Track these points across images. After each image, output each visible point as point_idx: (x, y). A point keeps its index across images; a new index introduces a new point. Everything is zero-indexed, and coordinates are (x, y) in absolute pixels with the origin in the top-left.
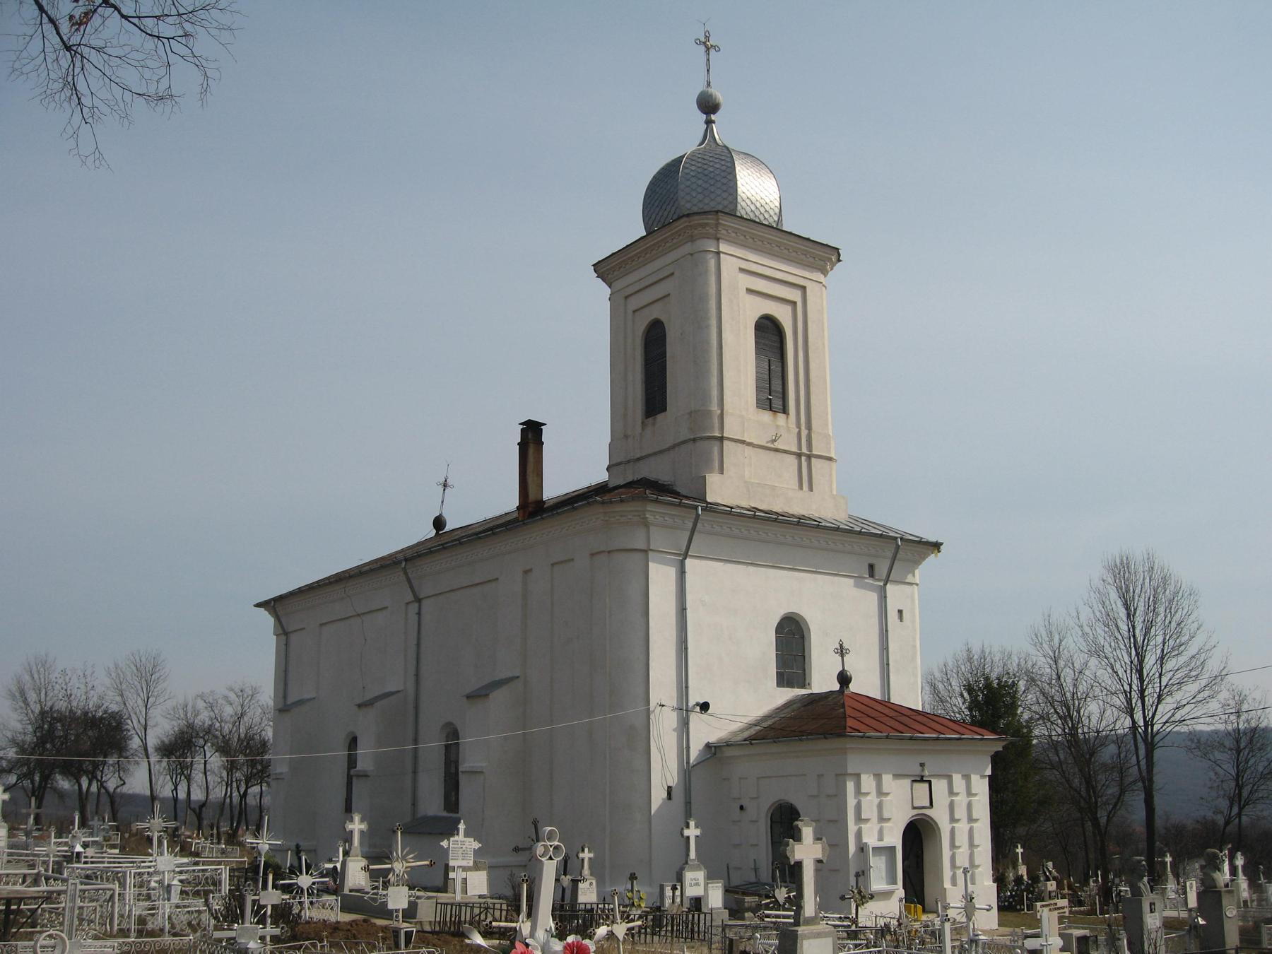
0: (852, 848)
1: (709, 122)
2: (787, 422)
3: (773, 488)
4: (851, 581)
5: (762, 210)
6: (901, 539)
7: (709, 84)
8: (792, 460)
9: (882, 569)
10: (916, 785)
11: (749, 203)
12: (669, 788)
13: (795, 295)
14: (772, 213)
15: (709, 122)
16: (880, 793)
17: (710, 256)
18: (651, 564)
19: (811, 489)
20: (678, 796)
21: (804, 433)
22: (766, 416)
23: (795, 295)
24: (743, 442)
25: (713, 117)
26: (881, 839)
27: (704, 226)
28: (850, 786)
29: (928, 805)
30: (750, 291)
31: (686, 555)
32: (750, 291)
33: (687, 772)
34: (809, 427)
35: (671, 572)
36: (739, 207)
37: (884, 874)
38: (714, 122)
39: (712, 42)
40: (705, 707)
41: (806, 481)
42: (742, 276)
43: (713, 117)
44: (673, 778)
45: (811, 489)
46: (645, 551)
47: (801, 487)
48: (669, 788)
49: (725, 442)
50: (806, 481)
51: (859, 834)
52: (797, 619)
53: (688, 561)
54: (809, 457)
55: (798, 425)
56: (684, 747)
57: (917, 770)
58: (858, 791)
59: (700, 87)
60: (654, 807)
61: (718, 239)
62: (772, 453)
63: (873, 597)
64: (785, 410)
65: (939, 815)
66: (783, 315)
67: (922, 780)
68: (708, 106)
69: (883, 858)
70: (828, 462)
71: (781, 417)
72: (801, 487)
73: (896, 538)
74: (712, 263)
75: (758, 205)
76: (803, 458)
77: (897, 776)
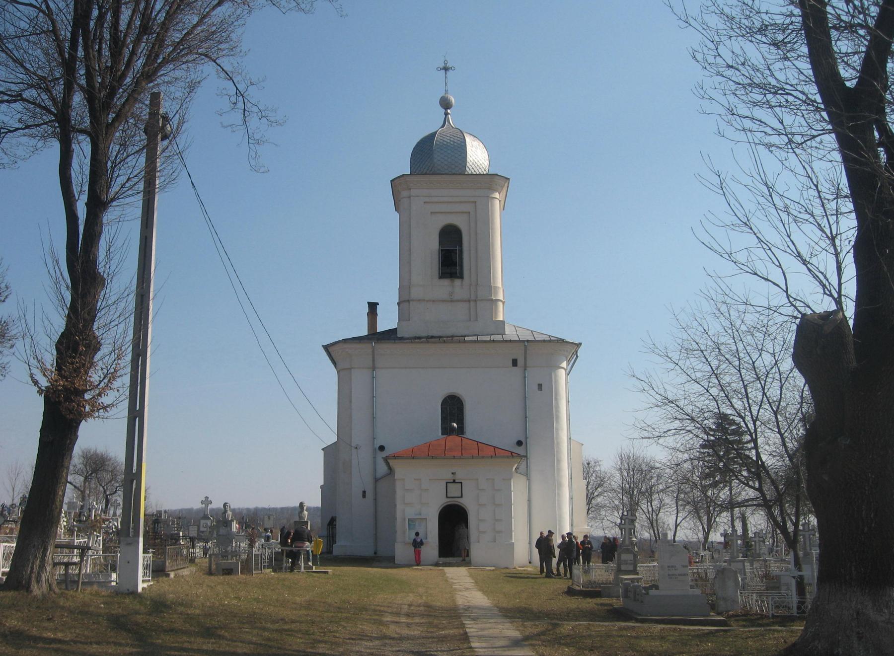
1: (446, 114)
2: (462, 283)
7: (446, 91)
9: (520, 362)
15: (446, 114)
20: (369, 494)
22: (446, 282)
25: (449, 111)
29: (460, 495)
31: (374, 368)
38: (449, 114)
40: (382, 448)
43: (449, 111)
46: (350, 369)
49: (411, 302)
52: (458, 396)
54: (475, 301)
57: (450, 477)
59: (443, 94)
61: (410, 189)
65: (467, 502)
66: (459, 221)
67: (454, 482)
68: (446, 104)
71: (457, 282)
76: (471, 302)
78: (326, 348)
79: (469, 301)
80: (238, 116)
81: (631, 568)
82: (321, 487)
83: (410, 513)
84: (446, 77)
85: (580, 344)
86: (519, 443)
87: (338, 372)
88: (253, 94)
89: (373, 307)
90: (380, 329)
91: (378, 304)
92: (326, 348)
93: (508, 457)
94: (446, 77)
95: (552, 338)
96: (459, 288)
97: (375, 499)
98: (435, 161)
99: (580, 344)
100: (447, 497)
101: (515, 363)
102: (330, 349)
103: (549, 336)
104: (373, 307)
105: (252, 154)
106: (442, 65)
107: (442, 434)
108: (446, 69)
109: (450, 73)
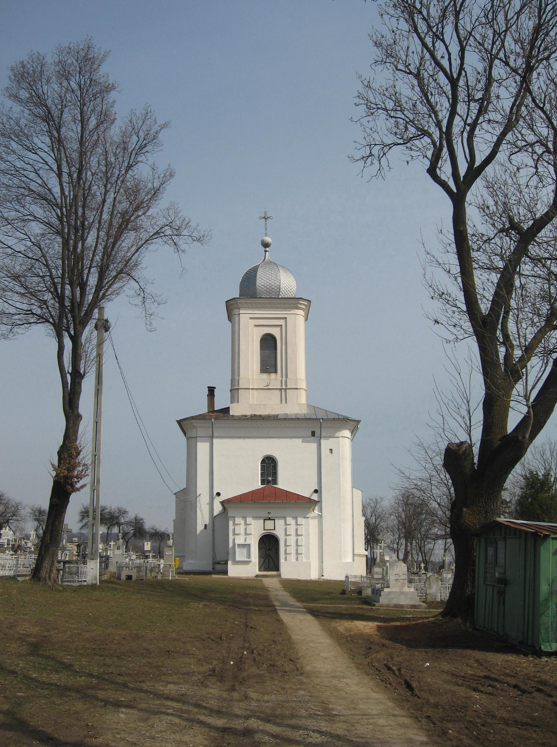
0: (231, 545)
3: (265, 405)
4: (300, 440)
5: (270, 288)
6: (322, 419)
8: (278, 392)
9: (317, 433)
10: (266, 522)
11: (263, 287)
12: (206, 525)
13: (282, 322)
14: (276, 288)
16: (246, 524)
17: (236, 316)
18: (198, 443)
19: (286, 403)
20: (209, 528)
21: (284, 379)
22: (265, 376)
23: (282, 322)
24: (249, 389)
25: (267, 249)
26: (245, 541)
27: (233, 304)
28: (231, 523)
30: (256, 326)
31: (212, 437)
32: (256, 326)
33: (213, 519)
34: (287, 377)
35: (207, 445)
36: (258, 290)
37: (246, 555)
39: (268, 215)
40: (218, 494)
41: (284, 399)
42: (250, 320)
44: (207, 521)
45: (286, 403)
46: (196, 437)
47: (281, 403)
48: (206, 525)
49: (240, 390)
50: (284, 399)
51: (234, 540)
53: (215, 441)
54: (286, 389)
55: (282, 377)
56: (212, 510)
57: (266, 515)
58: (234, 524)
60: (198, 532)
62: (267, 391)
63: (314, 446)
64: (276, 372)
65: (279, 533)
66: (275, 332)
67: (269, 519)
69: (246, 549)
70: (296, 390)
71: (273, 376)
72: (281, 403)
73: (319, 419)
74: (237, 319)
75: (268, 287)
77: (255, 518)
78: (179, 422)
79: (281, 389)
80: (139, 300)
81: (380, 576)
82: (174, 521)
83: (240, 540)
84: (266, 224)
85: (360, 421)
86: (316, 491)
87: (187, 439)
88: (149, 289)
89: (211, 390)
90: (216, 408)
91: (215, 388)
92: (179, 422)
93: (307, 502)
94: (266, 224)
95: (340, 417)
96: (274, 380)
97: (213, 530)
98: (257, 287)
99: (360, 421)
100: (264, 530)
101: (313, 434)
102: (182, 423)
103: (338, 415)
104: (211, 390)
105: (148, 322)
106: (263, 215)
107: (262, 484)
108: (265, 218)
109: (269, 220)
